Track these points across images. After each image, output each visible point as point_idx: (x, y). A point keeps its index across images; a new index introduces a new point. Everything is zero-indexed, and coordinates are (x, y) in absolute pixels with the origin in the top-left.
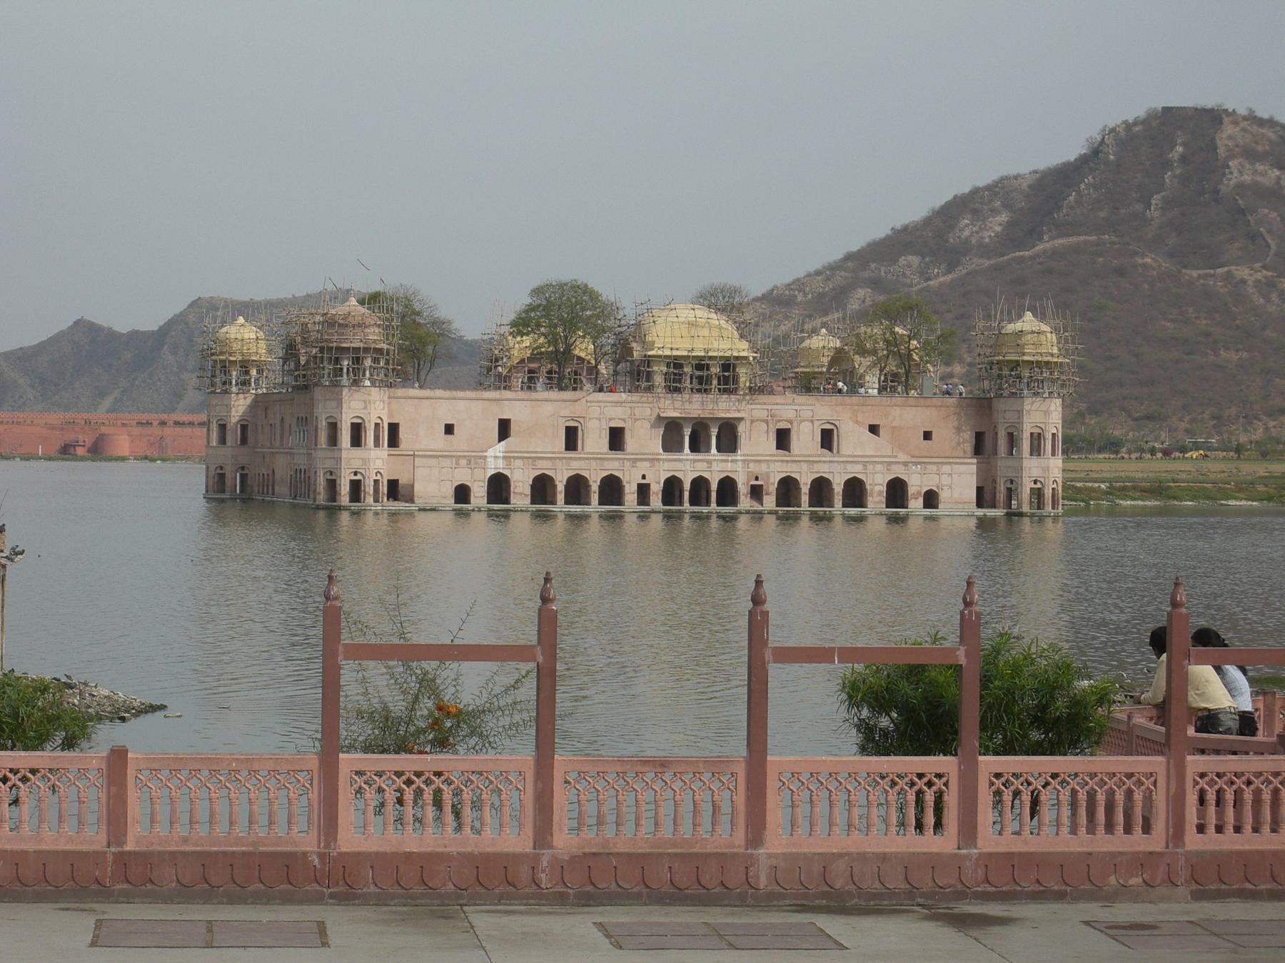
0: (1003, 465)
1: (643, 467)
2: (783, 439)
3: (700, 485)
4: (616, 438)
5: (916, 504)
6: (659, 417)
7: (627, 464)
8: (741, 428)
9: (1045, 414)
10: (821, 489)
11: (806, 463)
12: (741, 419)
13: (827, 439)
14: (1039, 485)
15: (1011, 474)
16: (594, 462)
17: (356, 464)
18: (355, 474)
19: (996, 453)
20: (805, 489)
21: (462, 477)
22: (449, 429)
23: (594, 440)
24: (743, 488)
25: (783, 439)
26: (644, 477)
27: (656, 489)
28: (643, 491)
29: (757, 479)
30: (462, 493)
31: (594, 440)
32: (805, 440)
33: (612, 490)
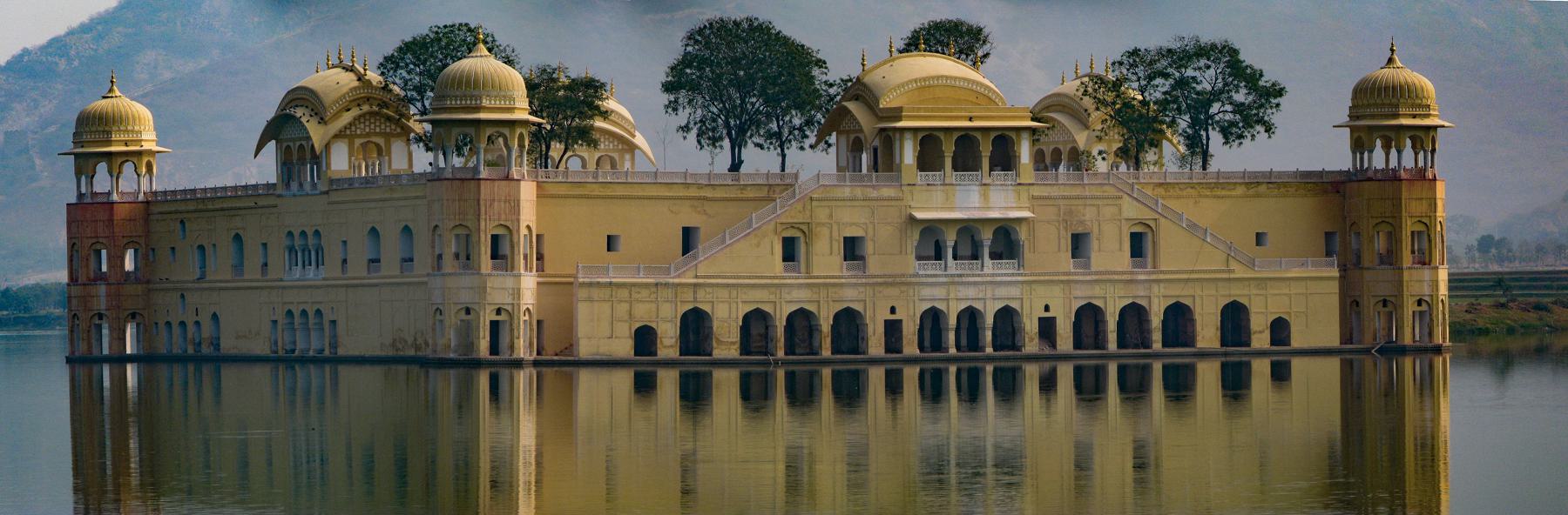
1: (892, 295)
2: (1078, 244)
4: (852, 249)
6: (912, 219)
7: (869, 291)
8: (1023, 234)
10: (1134, 315)
12: (1019, 220)
13: (1138, 245)
14: (1424, 307)
16: (823, 287)
17: (504, 299)
18: (499, 311)
19: (1358, 263)
20: (1156, 321)
21: (644, 313)
22: (611, 243)
24: (1031, 326)
25: (1078, 244)
30: (645, 338)
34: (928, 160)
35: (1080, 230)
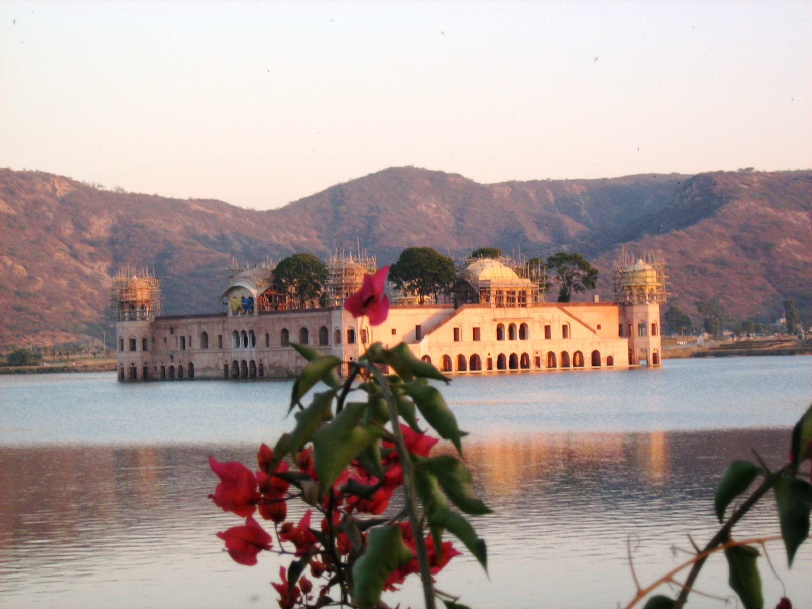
0: (637, 340)
2: (547, 329)
3: (513, 357)
4: (476, 333)
5: (604, 364)
9: (653, 313)
11: (558, 345)
15: (643, 346)
22: (394, 332)
23: (467, 335)
24: (532, 359)
25: (547, 329)
26: (489, 354)
27: (495, 361)
28: (490, 361)
29: (537, 353)
31: (467, 335)
32: (556, 332)
33: (475, 362)
34: (499, 299)
35: (547, 324)
